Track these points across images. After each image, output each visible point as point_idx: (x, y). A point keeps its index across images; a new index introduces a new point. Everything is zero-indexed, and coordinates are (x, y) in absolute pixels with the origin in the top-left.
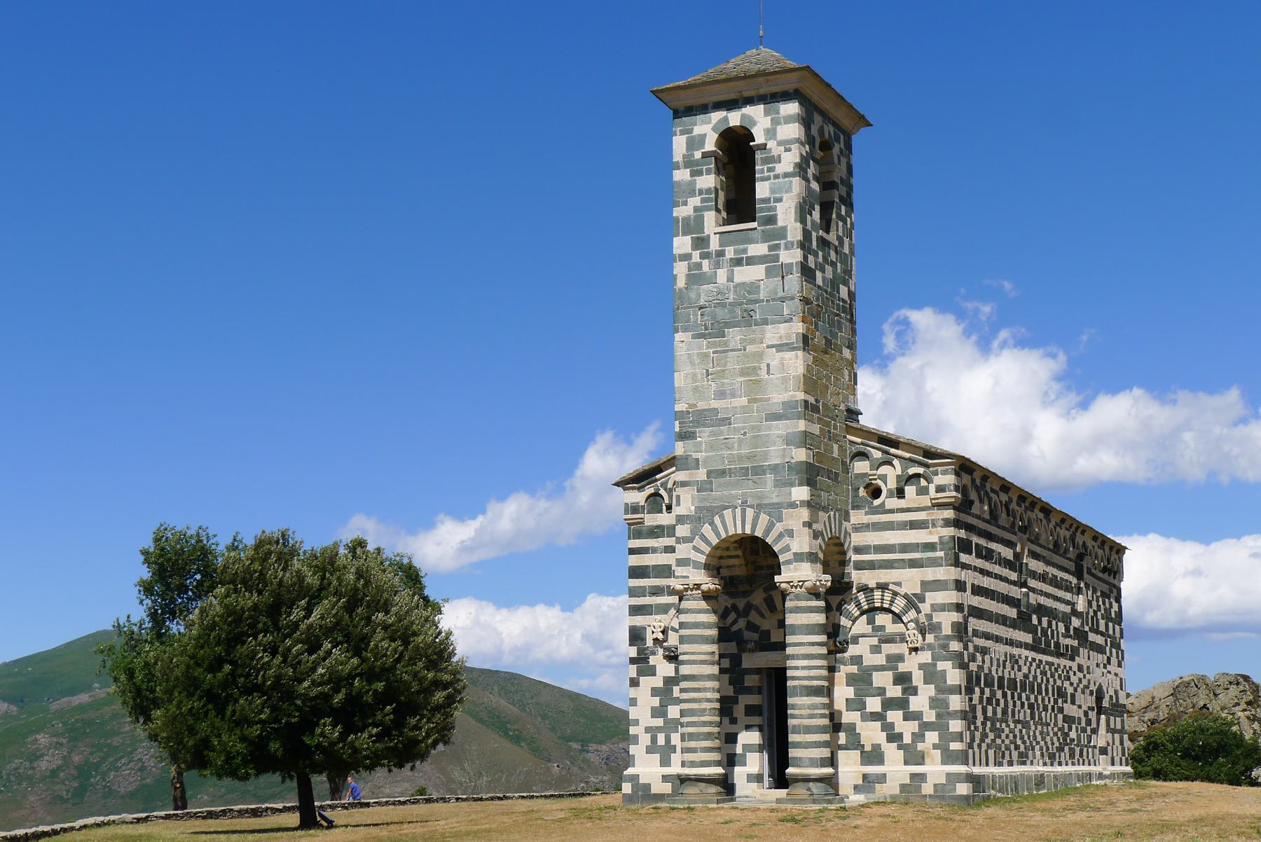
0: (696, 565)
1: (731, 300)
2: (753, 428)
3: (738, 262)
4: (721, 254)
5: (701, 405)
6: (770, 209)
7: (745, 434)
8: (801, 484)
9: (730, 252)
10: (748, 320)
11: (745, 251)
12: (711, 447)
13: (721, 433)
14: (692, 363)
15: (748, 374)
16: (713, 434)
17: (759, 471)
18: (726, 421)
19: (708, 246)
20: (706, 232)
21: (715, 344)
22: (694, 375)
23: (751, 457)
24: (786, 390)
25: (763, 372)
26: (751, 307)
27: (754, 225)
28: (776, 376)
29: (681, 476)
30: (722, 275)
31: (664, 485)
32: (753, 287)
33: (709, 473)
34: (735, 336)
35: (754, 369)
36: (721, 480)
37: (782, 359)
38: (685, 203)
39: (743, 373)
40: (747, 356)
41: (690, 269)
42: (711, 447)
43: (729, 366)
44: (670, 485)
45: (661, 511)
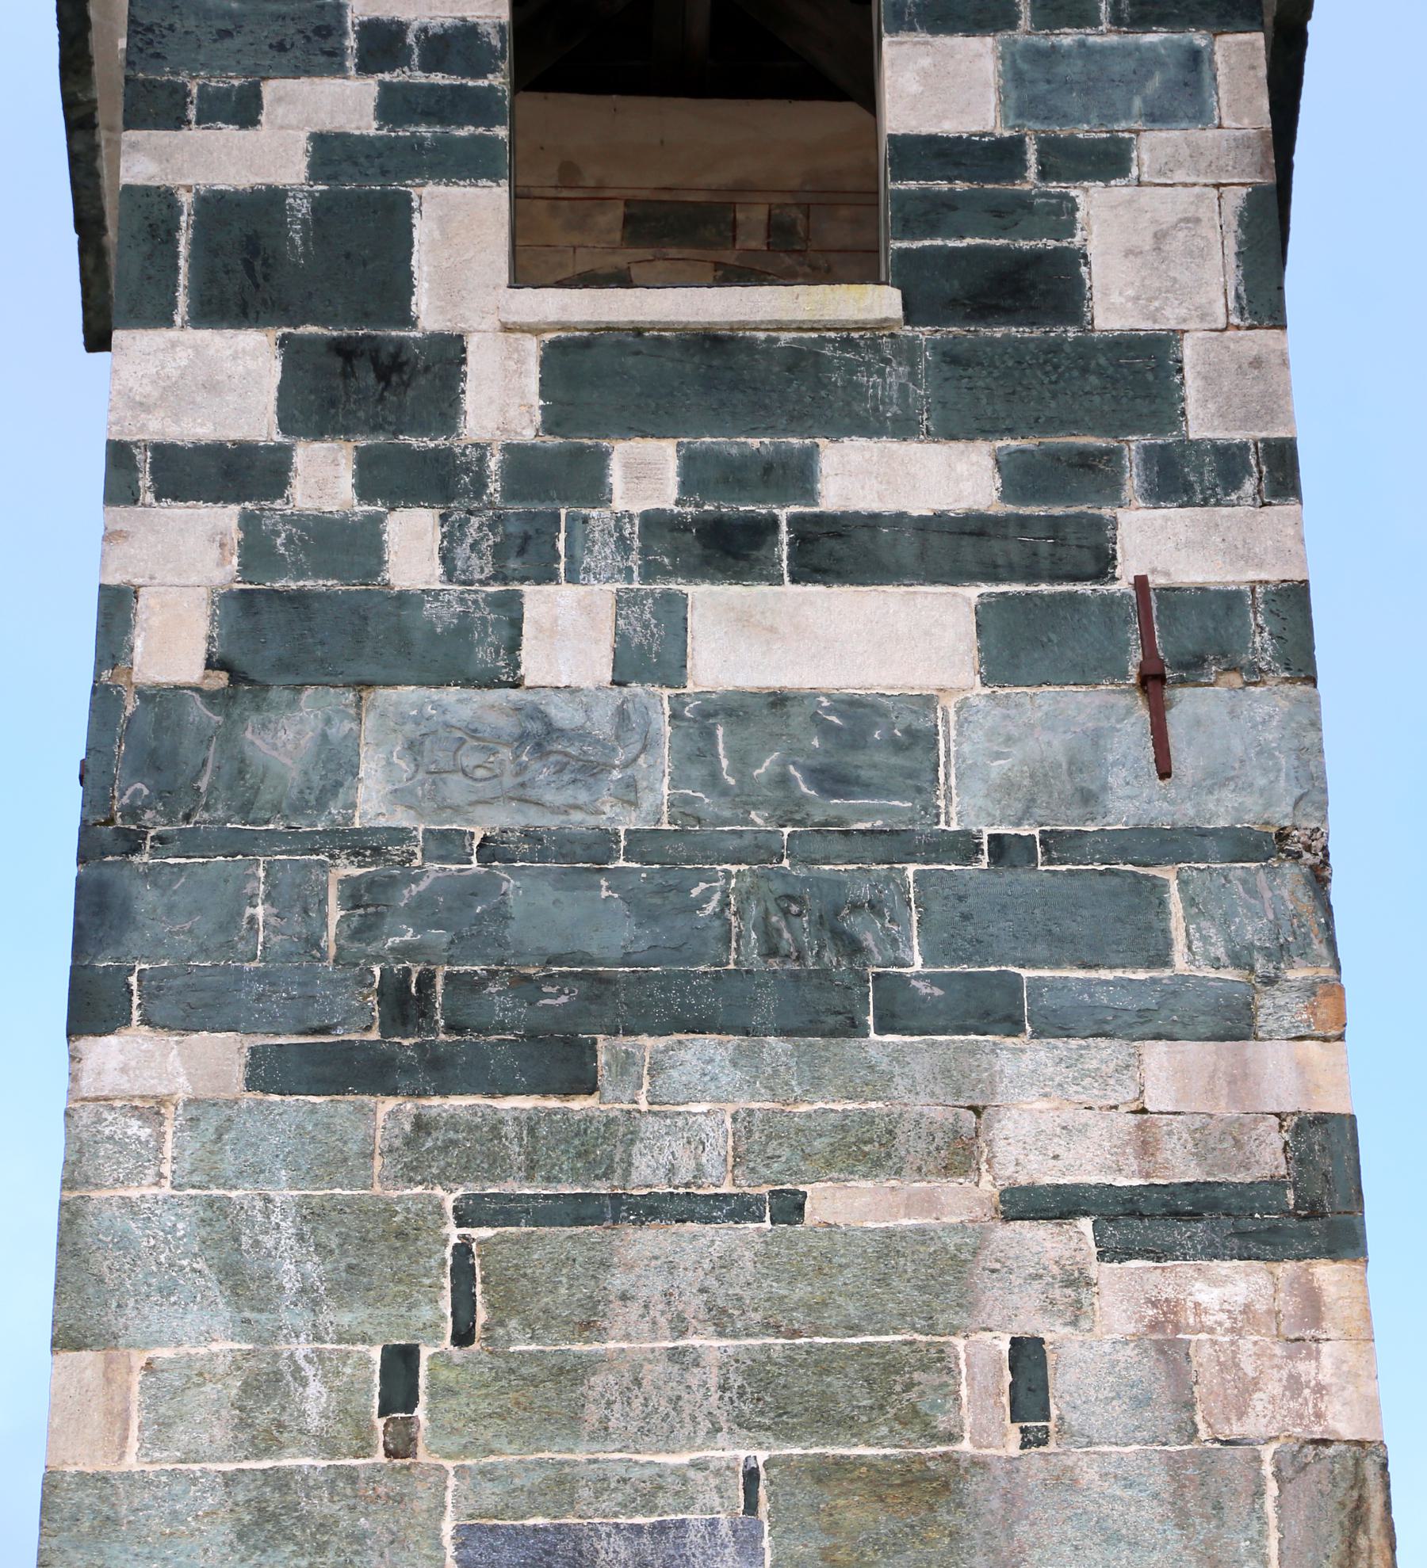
3: (726, 547)
4: (557, 475)
6: (1011, 212)
10: (822, 997)
11: (798, 475)
14: (242, 1282)
15: (827, 1419)
19: (445, 408)
20: (429, 312)
22: (266, 1384)
25: (983, 1429)
27: (880, 302)
32: (865, 740)
35: (884, 1371)
37: (1165, 1337)
38: (244, 110)
39: (767, 1397)
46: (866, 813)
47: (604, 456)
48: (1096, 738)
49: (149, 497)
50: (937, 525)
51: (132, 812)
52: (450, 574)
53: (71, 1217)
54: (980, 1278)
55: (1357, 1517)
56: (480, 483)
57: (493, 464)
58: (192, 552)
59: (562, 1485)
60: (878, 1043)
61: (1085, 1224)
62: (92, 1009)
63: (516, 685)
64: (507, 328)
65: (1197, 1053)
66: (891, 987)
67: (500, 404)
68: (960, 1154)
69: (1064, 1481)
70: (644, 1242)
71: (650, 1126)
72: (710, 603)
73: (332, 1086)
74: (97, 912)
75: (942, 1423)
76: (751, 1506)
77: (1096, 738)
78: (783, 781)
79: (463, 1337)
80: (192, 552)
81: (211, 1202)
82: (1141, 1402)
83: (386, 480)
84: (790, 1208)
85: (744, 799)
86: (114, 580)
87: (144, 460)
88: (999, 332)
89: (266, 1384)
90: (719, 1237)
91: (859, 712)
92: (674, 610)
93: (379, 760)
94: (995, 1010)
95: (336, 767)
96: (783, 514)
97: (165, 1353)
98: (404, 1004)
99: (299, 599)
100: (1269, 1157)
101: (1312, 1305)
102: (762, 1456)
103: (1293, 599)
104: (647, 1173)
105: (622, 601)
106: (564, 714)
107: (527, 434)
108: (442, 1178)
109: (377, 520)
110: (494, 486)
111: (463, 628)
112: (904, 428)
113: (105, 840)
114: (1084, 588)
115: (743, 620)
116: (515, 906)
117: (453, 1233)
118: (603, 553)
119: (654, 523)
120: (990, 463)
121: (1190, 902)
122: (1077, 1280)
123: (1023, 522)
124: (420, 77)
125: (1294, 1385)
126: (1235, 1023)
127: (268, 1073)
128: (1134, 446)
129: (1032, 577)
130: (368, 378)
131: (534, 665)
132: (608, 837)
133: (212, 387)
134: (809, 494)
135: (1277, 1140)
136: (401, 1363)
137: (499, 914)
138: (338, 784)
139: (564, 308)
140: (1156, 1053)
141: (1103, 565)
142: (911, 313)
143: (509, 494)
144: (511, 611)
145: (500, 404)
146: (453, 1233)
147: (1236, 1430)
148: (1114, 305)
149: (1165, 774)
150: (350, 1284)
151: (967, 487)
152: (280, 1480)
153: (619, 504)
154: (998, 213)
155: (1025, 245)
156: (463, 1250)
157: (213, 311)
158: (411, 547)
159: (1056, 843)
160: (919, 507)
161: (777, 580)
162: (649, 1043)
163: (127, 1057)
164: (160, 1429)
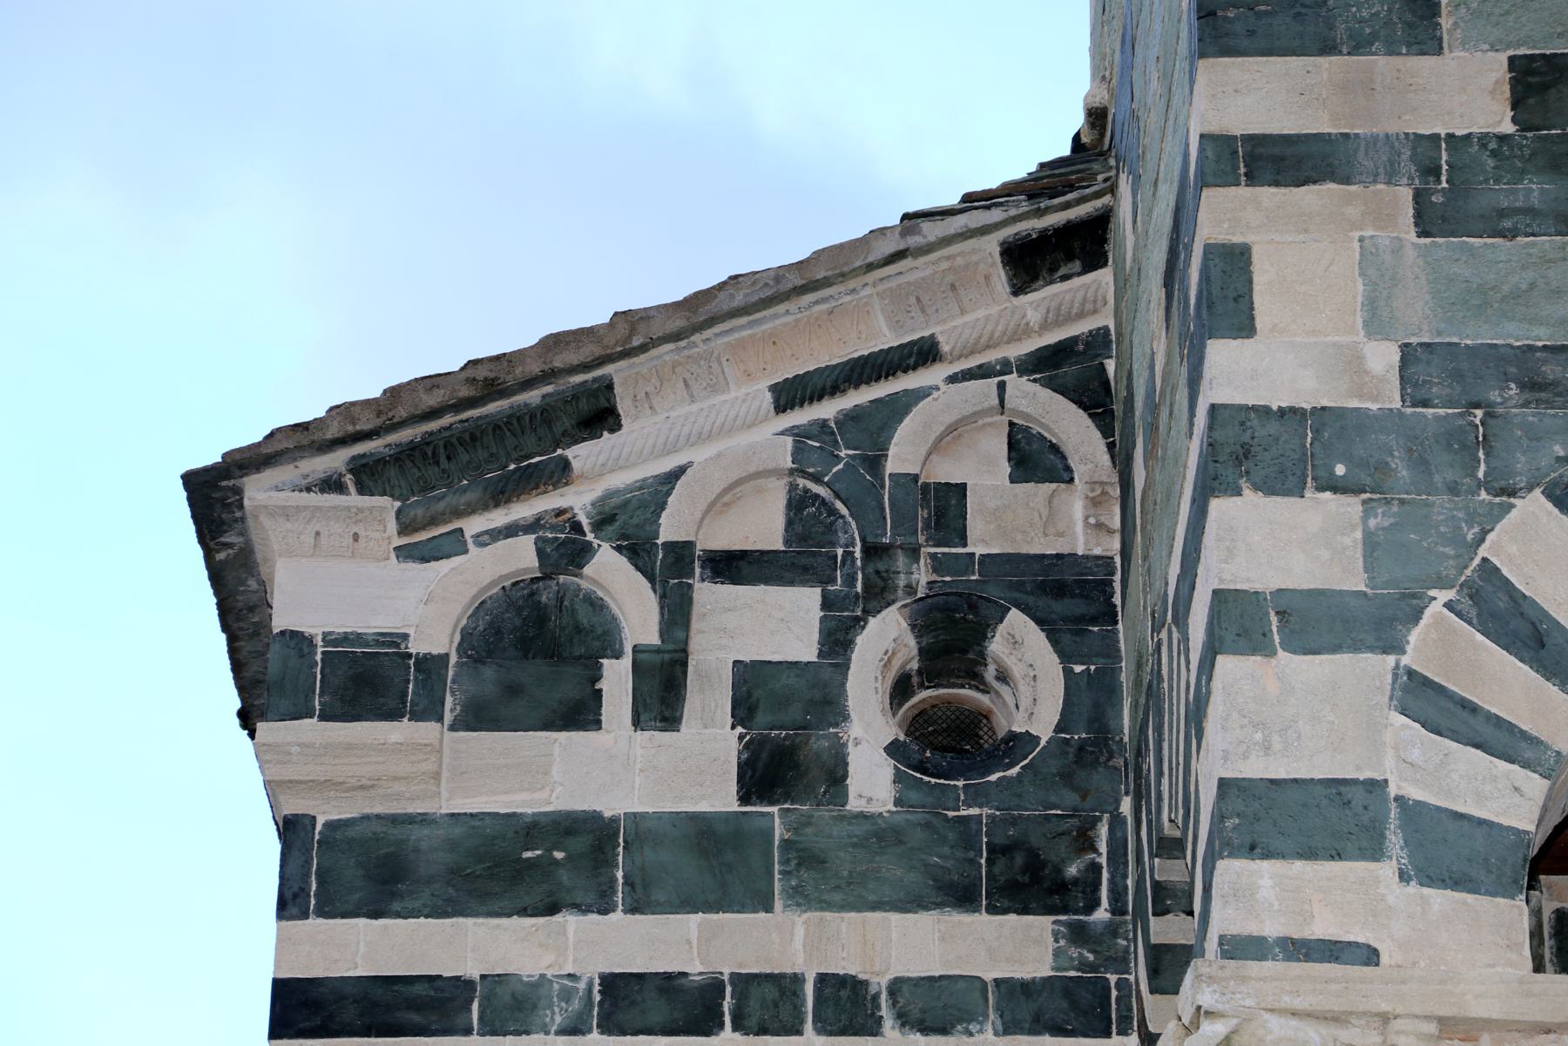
0: (1447, 852)
44: (670, 529)
45: (581, 713)
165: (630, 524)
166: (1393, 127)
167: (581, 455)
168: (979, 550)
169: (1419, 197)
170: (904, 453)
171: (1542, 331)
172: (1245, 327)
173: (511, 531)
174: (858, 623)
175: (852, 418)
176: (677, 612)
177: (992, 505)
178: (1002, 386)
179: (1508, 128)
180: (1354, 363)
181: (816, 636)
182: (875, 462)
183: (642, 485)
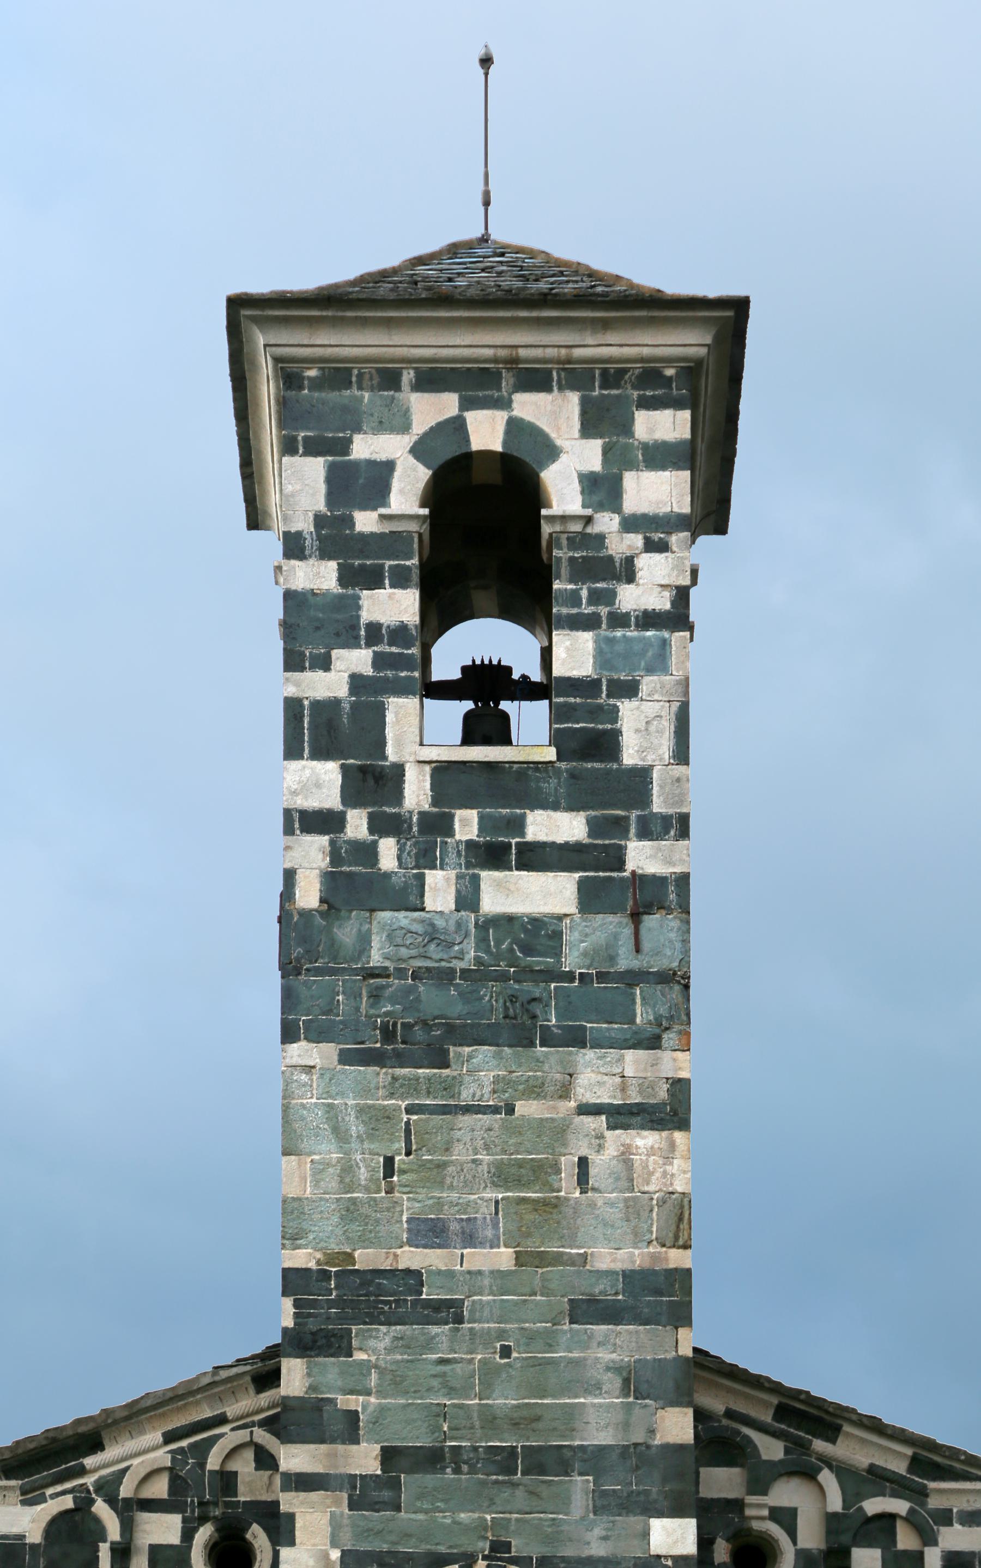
1: (469, 962)
2: (530, 1338)
4: (437, 824)
5: (365, 1258)
7: (506, 1352)
8: (677, 1512)
9: (467, 825)
11: (518, 825)
12: (395, 1381)
13: (429, 1344)
15: (519, 1183)
16: (400, 1343)
17: (550, 1462)
18: (448, 1311)
19: (397, 795)
20: (392, 754)
21: (412, 1087)
22: (347, 1169)
23: (525, 1420)
24: (638, 1238)
26: (530, 988)
28: (607, 1197)
29: (295, 1458)
30: (440, 889)
31: (108, 1489)
32: (539, 933)
33: (389, 1456)
34: (480, 1070)
36: (429, 1480)
39: (503, 1176)
40: (516, 1131)
41: (335, 856)
42: (395, 1381)
43: (460, 1154)
44: (126, 1491)
46: (539, 962)
47: (452, 817)
48: (616, 936)
49: (298, 832)
50: (566, 847)
51: (298, 960)
52: (400, 866)
53: (286, 1109)
54: (571, 1137)
55: (680, 1219)
56: (410, 828)
57: (415, 819)
58: (313, 852)
59: (439, 1204)
60: (540, 1050)
61: (604, 1117)
62: (289, 1034)
63: (423, 909)
64: (419, 762)
65: (641, 1053)
66: (545, 1029)
67: (417, 793)
68: (565, 1092)
69: (592, 1205)
70: (465, 1120)
71: (467, 1079)
72: (488, 877)
73: (366, 1063)
74: (289, 999)
75: (556, 1186)
76: (497, 1213)
77: (616, 936)
78: (511, 950)
79: (408, 1153)
80: (313, 852)
81: (329, 1105)
82: (618, 1179)
83: (380, 825)
84: (510, 1110)
85: (498, 957)
86: (288, 865)
87: (296, 816)
88: (589, 765)
89: (347, 1169)
90: (486, 1119)
91: (536, 922)
92: (476, 880)
93: (380, 938)
94: (577, 1039)
95: (364, 941)
96: (513, 841)
97: (316, 1157)
98: (388, 1034)
99: (350, 875)
100: (662, 1093)
101: (672, 1145)
102: (500, 1196)
103: (683, 880)
104: (466, 1096)
105: (458, 877)
106: (440, 923)
107: (426, 807)
108: (402, 1098)
109: (375, 843)
110: (415, 829)
111: (406, 887)
112: (555, 807)
113: (289, 968)
114: (615, 874)
115: (499, 884)
116: (423, 997)
117: (405, 1118)
118: (452, 858)
119: (470, 844)
120: (584, 821)
121: (643, 999)
122: (601, 1137)
123: (596, 846)
124: (387, 649)
125: (665, 1174)
126: (653, 1043)
127: (345, 1058)
128: (634, 814)
129: (597, 870)
130: (371, 782)
131: (429, 904)
132: (453, 970)
133: (318, 785)
134: (522, 834)
135: (666, 1087)
136: (389, 1161)
137: (418, 1000)
138: (365, 949)
139: (439, 755)
140: (630, 1055)
141: (620, 864)
142: (560, 758)
143: (420, 831)
144: (421, 879)
145: (417, 793)
146: (405, 1118)
147: (646, 1189)
148: (630, 757)
149: (638, 950)
150: (371, 1135)
151: (576, 831)
152: (353, 1201)
153: (458, 837)
154: (591, 712)
155: (600, 727)
156: (408, 1123)
157: (320, 754)
158: (388, 853)
159: (602, 976)
160: (560, 839)
161: (510, 869)
162: (467, 1050)
163: (300, 1052)
164: (316, 1183)
165: (108, 1489)
166: (342, 1470)
167: (89, 1462)
168: (242, 1499)
169: (350, 1497)
170: (213, 1462)
171: (385, 1546)
172: (292, 1543)
173: (63, 1493)
174: (195, 1530)
175: (193, 1446)
176: (128, 1526)
177: (247, 1479)
178: (252, 1432)
179: (379, 1472)
180: (326, 1556)
181: (179, 1534)
182: (202, 1465)
183: (113, 1473)
